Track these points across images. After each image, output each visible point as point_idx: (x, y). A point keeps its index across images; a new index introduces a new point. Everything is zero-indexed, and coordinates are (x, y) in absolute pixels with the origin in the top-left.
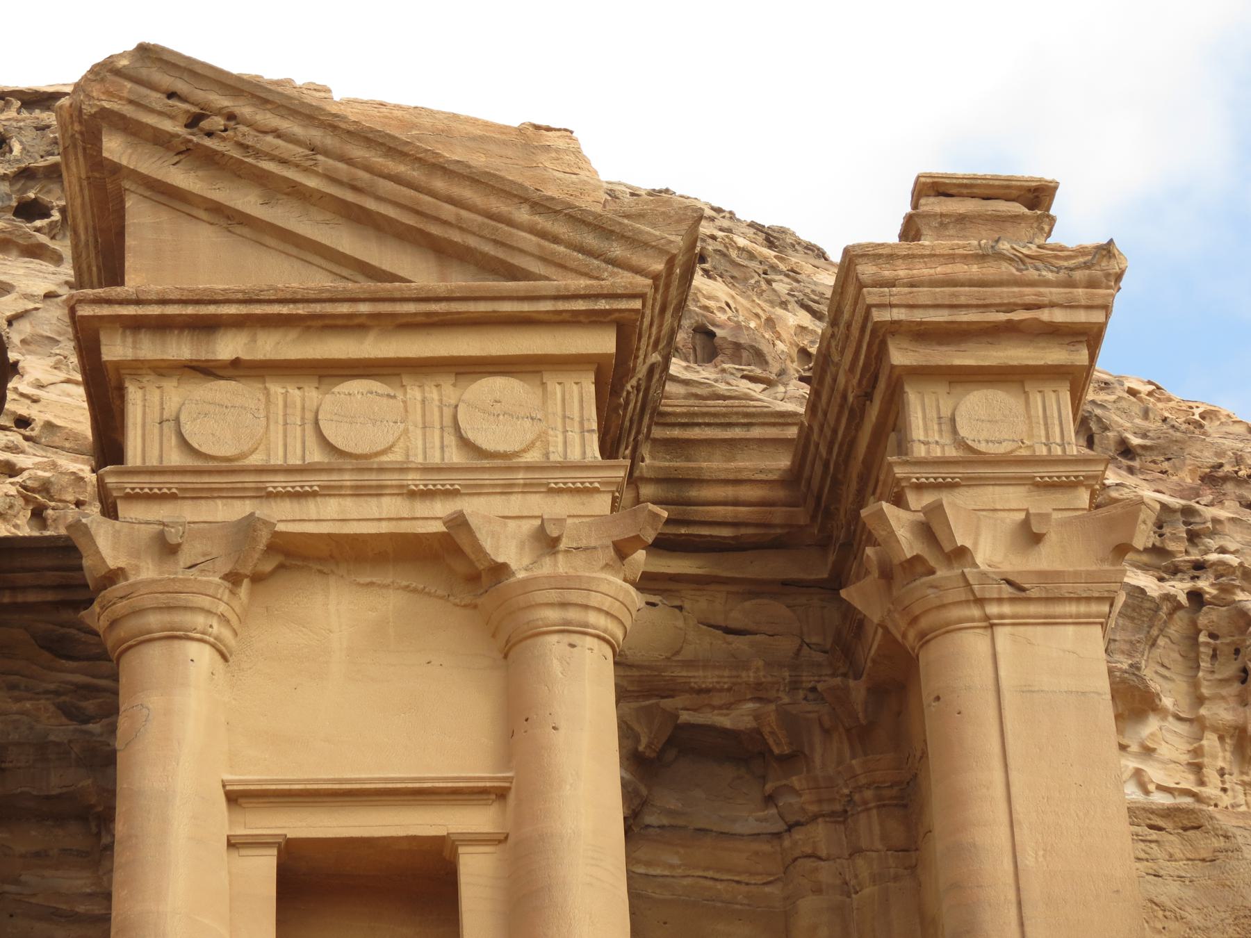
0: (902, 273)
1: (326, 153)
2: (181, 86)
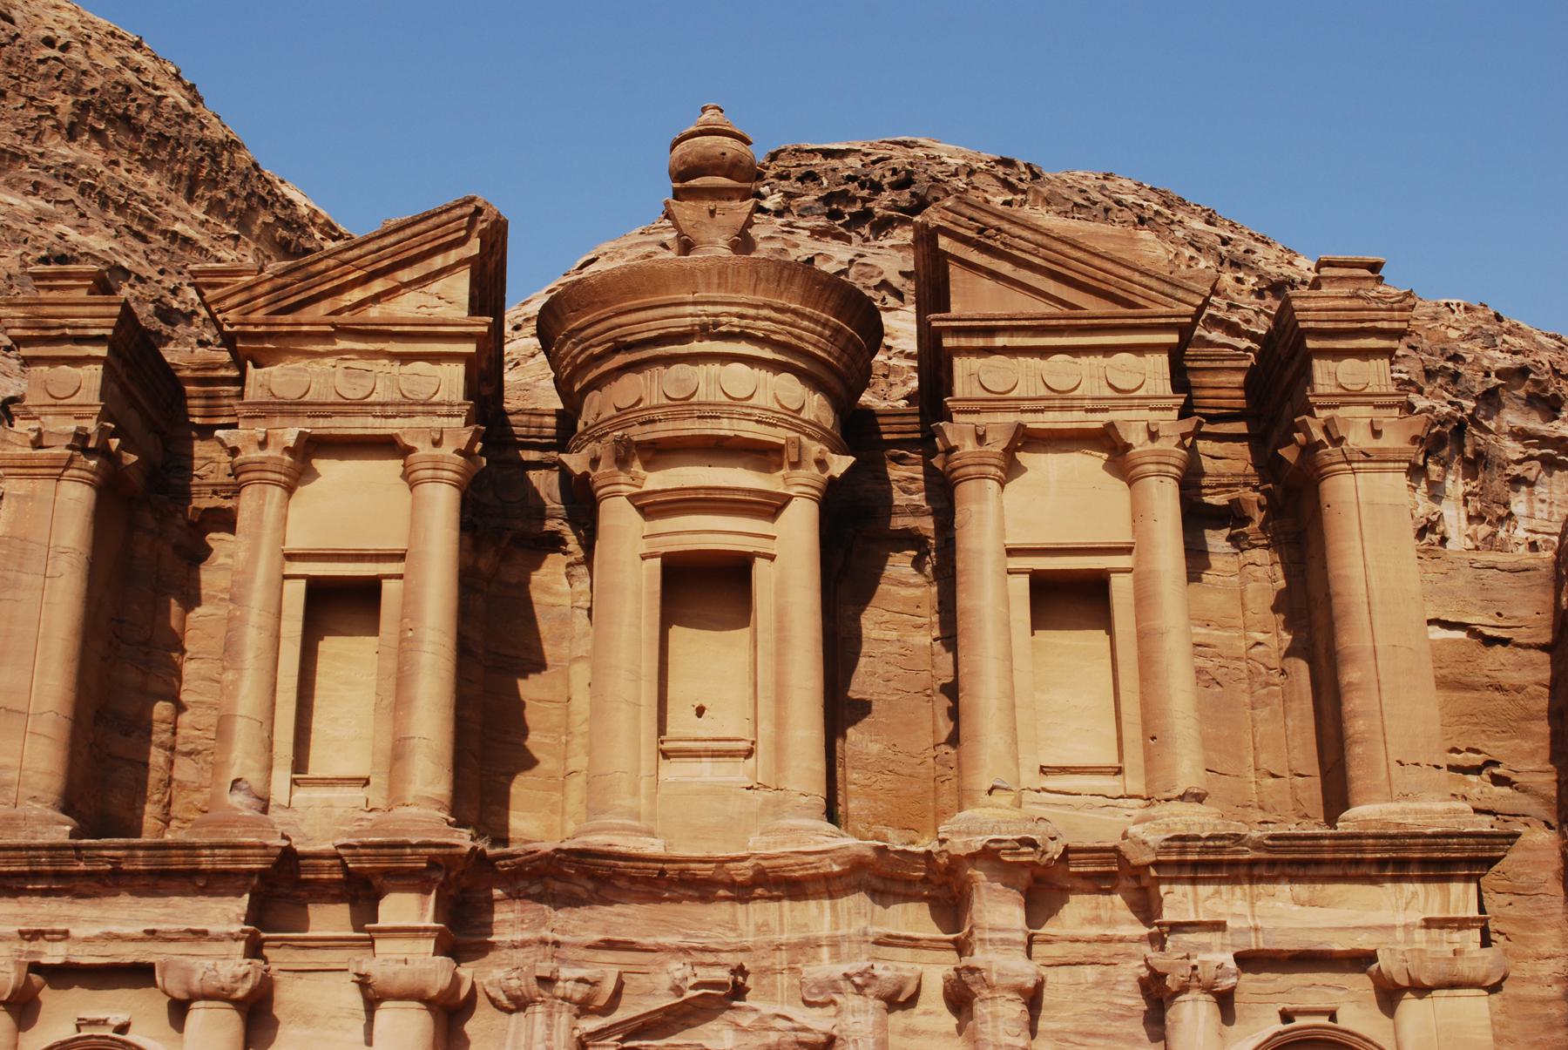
0: (1313, 305)
1: (1044, 247)
2: (976, 215)
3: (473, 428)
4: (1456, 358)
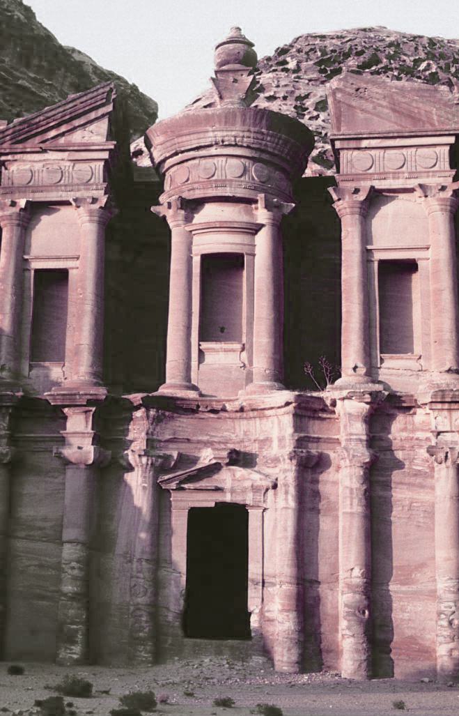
3: (107, 196)
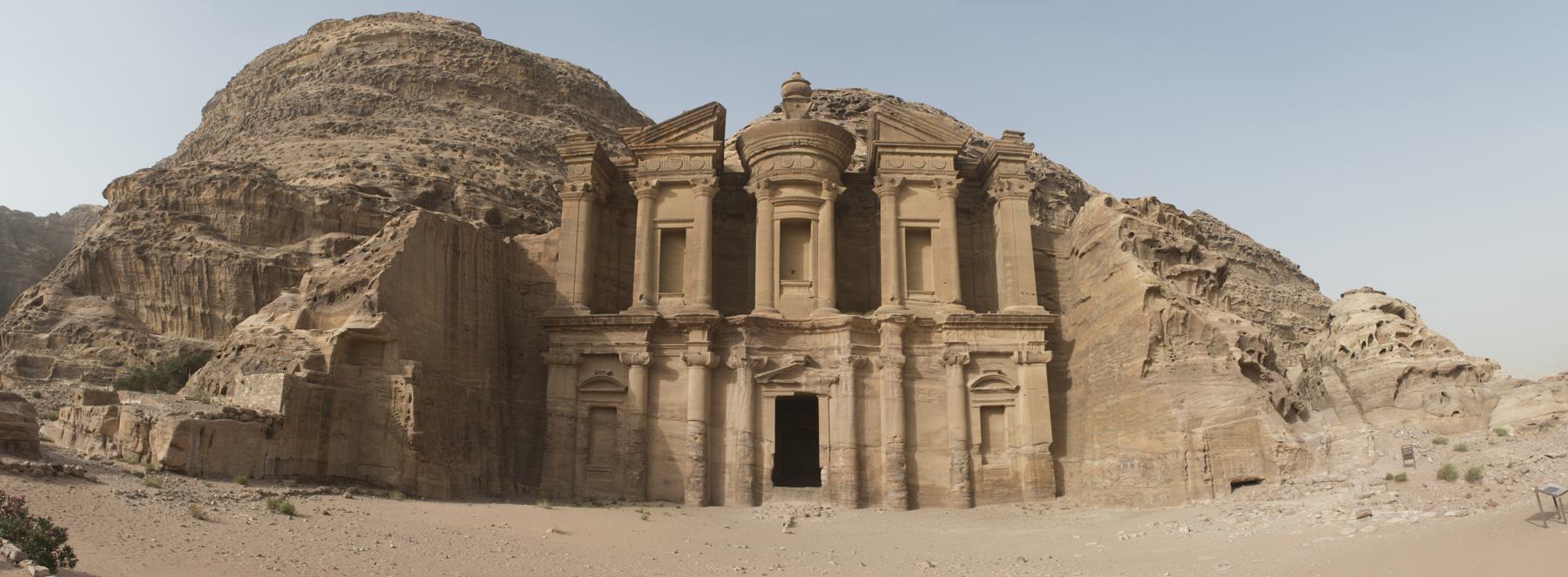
4: (1033, 168)
